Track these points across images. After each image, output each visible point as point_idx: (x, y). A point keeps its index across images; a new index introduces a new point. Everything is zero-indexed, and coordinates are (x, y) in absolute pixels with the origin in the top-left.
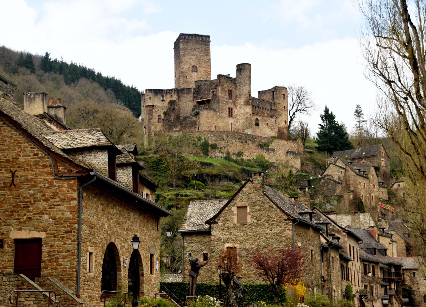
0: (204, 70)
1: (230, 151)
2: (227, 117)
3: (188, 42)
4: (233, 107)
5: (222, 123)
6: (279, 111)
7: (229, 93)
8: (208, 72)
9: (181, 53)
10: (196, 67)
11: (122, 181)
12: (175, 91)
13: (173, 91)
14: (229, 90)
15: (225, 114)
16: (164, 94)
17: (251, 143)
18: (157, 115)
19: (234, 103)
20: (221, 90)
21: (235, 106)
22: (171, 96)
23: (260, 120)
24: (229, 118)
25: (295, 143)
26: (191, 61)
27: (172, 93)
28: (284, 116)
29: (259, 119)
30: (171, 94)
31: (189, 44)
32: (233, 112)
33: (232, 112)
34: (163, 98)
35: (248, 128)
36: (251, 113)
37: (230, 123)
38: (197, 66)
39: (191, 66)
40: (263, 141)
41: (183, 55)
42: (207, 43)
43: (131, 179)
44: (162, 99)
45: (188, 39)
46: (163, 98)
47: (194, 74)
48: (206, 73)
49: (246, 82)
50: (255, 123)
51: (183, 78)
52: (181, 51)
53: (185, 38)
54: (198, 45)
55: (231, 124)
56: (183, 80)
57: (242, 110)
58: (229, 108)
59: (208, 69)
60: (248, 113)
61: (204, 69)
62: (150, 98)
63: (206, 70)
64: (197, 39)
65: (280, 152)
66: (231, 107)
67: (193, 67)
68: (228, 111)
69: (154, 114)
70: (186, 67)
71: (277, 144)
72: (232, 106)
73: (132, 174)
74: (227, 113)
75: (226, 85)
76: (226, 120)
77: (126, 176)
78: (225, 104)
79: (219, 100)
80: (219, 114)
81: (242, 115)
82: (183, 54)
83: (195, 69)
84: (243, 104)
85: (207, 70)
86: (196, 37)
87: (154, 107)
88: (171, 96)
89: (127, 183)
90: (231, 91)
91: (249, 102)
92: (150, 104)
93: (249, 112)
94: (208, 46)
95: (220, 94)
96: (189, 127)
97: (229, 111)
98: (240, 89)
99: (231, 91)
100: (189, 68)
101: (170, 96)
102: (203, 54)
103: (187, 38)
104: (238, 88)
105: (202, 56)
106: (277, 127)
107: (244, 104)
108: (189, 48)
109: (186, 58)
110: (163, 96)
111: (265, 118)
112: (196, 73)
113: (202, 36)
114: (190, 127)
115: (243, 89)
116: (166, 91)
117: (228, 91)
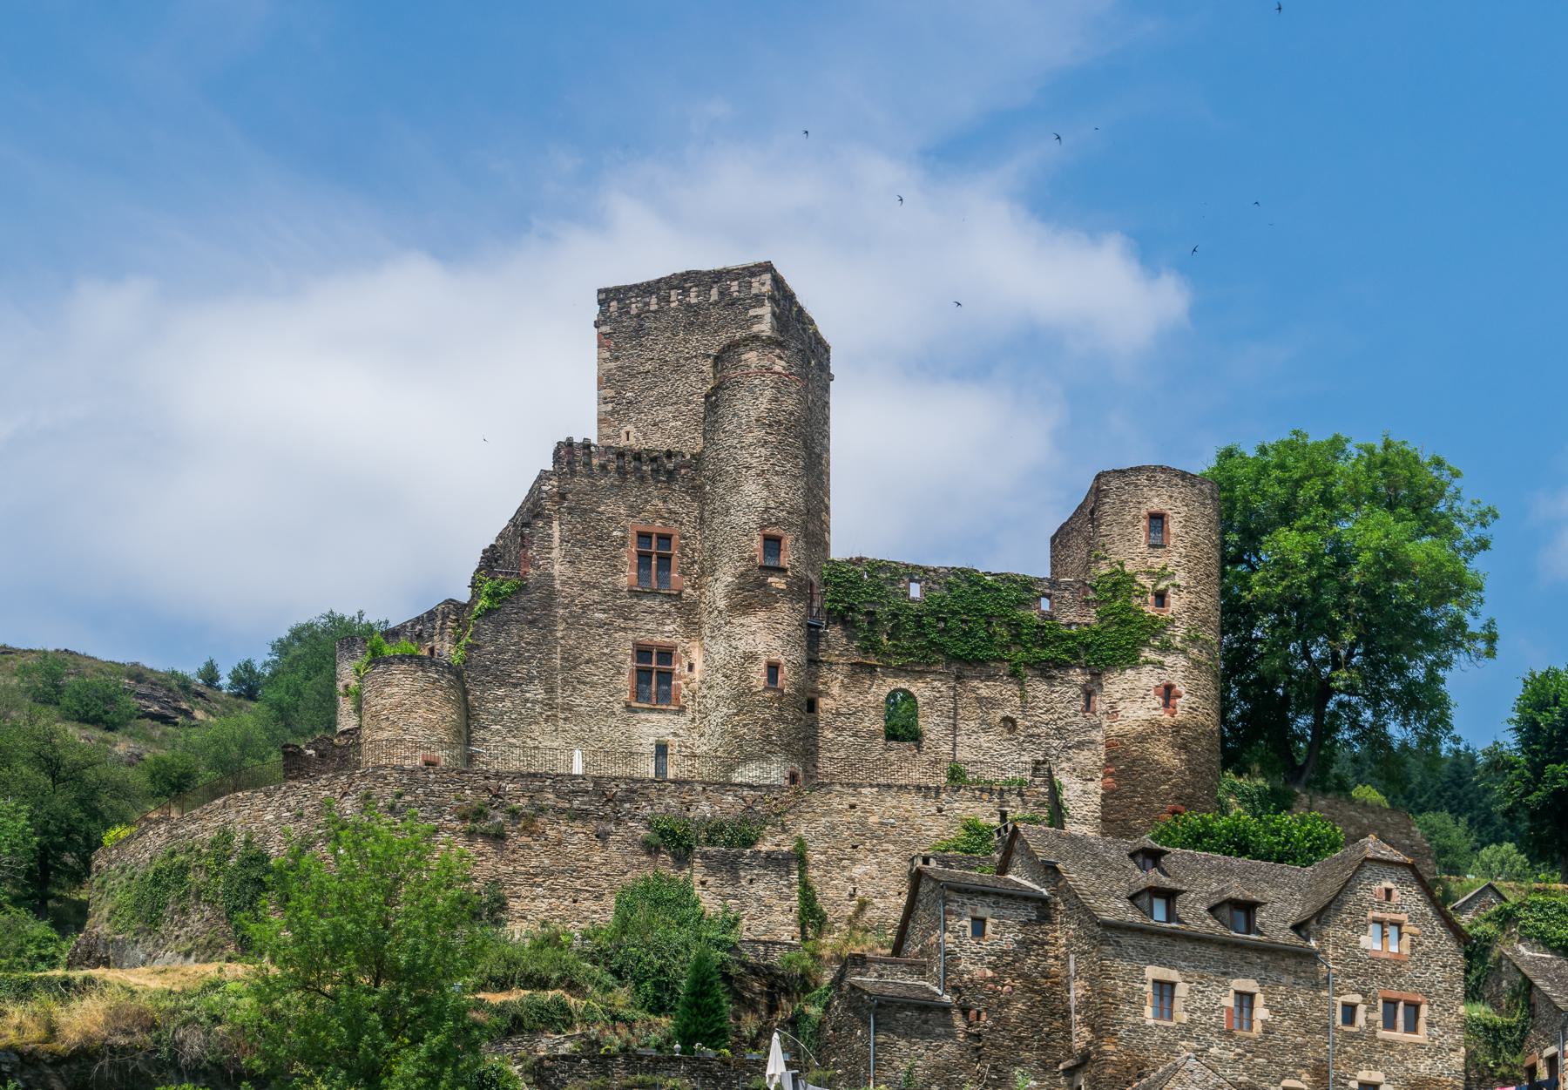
2: (617, 707)
3: (639, 332)
4: (676, 640)
7: (644, 558)
12: (445, 616)
14: (644, 537)
15: (602, 691)
17: (577, 836)
21: (692, 626)
23: (930, 704)
32: (679, 668)
35: (747, 759)
37: (652, 740)
40: (704, 809)
42: (752, 312)
53: (624, 310)
58: (642, 652)
60: (751, 657)
64: (694, 301)
66: (658, 639)
68: (629, 665)
72: (668, 632)
74: (626, 681)
78: (601, 624)
80: (550, 690)
81: (719, 678)
84: (722, 604)
86: (686, 292)
90: (665, 539)
91: (763, 585)
93: (761, 649)
95: (557, 569)
97: (642, 675)
99: (665, 539)
103: (634, 311)
106: (1098, 736)
108: (648, 366)
113: (718, 276)
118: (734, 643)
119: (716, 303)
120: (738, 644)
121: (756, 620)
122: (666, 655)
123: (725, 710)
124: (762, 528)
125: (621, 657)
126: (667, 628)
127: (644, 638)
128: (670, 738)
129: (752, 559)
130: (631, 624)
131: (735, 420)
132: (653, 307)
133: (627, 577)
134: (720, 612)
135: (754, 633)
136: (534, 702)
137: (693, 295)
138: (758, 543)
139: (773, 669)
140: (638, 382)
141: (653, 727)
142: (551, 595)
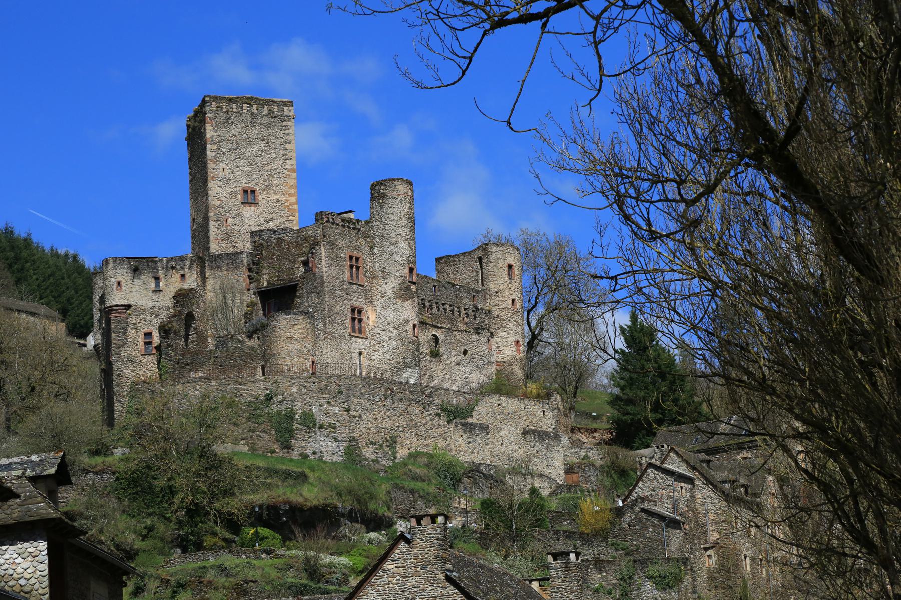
0: (278, 201)
1: (357, 434)
2: (347, 335)
3: (227, 121)
4: (364, 306)
5: (334, 353)
6: (497, 313)
7: (351, 267)
8: (288, 204)
9: (209, 154)
10: (253, 192)
11: (15, 576)
13: (188, 264)
14: (351, 258)
15: (341, 328)
16: (161, 274)
18: (142, 333)
19: (366, 292)
20: (329, 258)
21: (370, 301)
22: (183, 276)
24: (354, 339)
25: (547, 407)
26: (239, 174)
27: (183, 269)
28: (514, 328)
29: (440, 336)
30: (182, 273)
31: (232, 127)
32: (365, 319)
33: (360, 321)
34: (157, 285)
35: (408, 367)
36: (417, 323)
37: (358, 351)
38: (256, 187)
39: (239, 189)
41: (215, 157)
42: (285, 124)
43: (44, 567)
44: (153, 285)
45: (227, 112)
46: (157, 285)
47: (248, 212)
48: (282, 208)
49: (400, 231)
50: (428, 351)
51: (216, 224)
52: (208, 146)
53: (219, 108)
54: (258, 128)
55: (360, 354)
56: (215, 230)
57: (390, 315)
58: (353, 310)
59: (290, 195)
60: (407, 322)
61: (277, 197)
62: (119, 284)
63: (283, 199)
64: (255, 112)
65: (503, 433)
66: (358, 305)
67: (245, 192)
68: (349, 316)
69: (131, 333)
70: (225, 192)
71: (497, 409)
72: (360, 302)
73: (46, 552)
74: (348, 323)
75: (341, 243)
76: (345, 345)
77: (30, 559)
79: (322, 284)
80: (325, 326)
82: (214, 154)
83: (249, 196)
84: (391, 295)
85: (287, 201)
87: (130, 312)
88: (183, 276)
89: (33, 581)
91: (410, 289)
92: (119, 303)
93: (410, 318)
94: (287, 132)
95: (325, 270)
96: (234, 366)
97: (353, 320)
98: (383, 253)
99: (357, 259)
100: (232, 195)
101: (178, 276)
102: (273, 155)
103: (224, 110)
104: (376, 251)
105: (271, 160)
107: (397, 298)
108: (233, 138)
109: (224, 166)
110: (157, 279)
111: (458, 336)
112: (253, 208)
114: (240, 368)
115: (392, 254)
116: (165, 264)
117: (348, 259)
118: (399, 314)
119: (267, 115)
120: (401, 314)
121: (408, 305)
122: (360, 312)
123: (395, 343)
124: (409, 264)
125: (347, 312)
126: (361, 300)
127: (354, 305)
128: (363, 351)
129: (405, 277)
130: (349, 297)
131: (395, 214)
132: (235, 110)
133: (347, 277)
134: (390, 298)
135: (407, 311)
136: (320, 330)
137: (255, 109)
138: (407, 271)
139: (415, 326)
140: (227, 145)
141: (359, 345)
142: (323, 282)
